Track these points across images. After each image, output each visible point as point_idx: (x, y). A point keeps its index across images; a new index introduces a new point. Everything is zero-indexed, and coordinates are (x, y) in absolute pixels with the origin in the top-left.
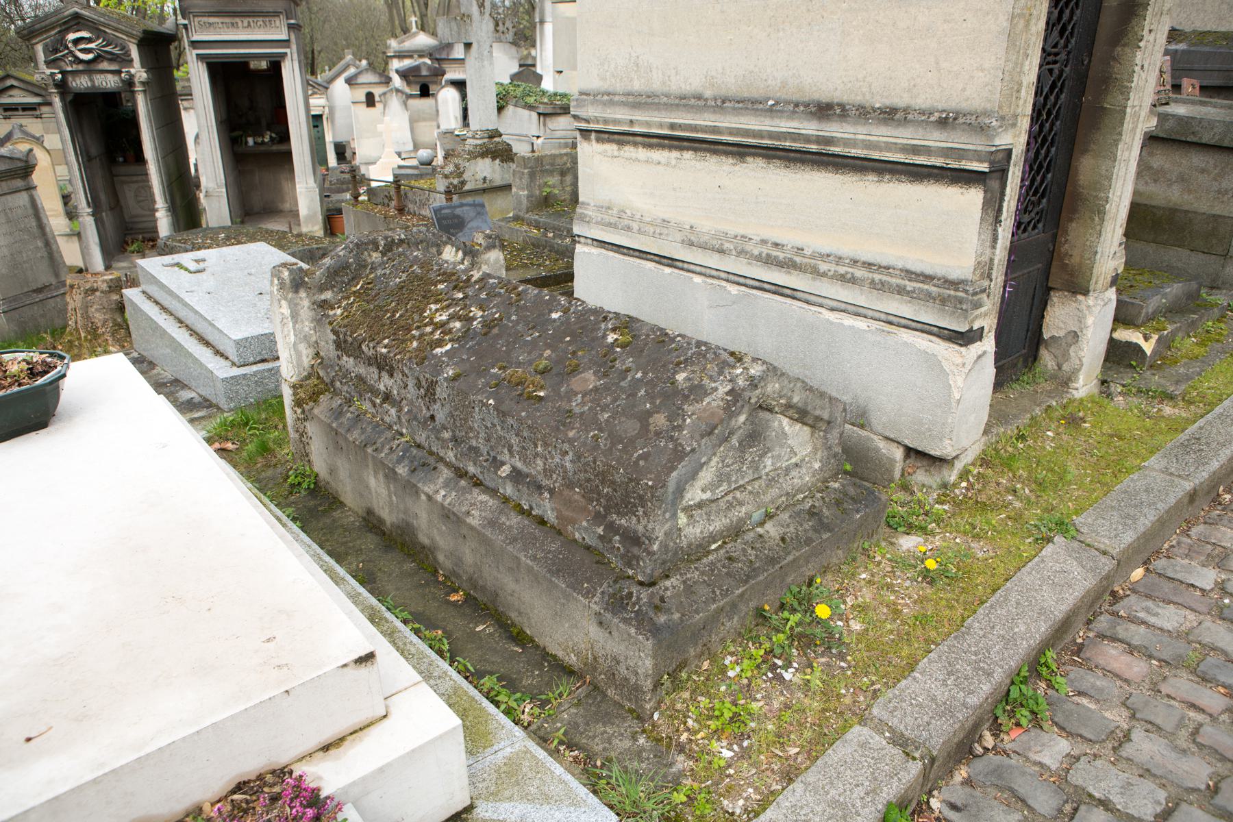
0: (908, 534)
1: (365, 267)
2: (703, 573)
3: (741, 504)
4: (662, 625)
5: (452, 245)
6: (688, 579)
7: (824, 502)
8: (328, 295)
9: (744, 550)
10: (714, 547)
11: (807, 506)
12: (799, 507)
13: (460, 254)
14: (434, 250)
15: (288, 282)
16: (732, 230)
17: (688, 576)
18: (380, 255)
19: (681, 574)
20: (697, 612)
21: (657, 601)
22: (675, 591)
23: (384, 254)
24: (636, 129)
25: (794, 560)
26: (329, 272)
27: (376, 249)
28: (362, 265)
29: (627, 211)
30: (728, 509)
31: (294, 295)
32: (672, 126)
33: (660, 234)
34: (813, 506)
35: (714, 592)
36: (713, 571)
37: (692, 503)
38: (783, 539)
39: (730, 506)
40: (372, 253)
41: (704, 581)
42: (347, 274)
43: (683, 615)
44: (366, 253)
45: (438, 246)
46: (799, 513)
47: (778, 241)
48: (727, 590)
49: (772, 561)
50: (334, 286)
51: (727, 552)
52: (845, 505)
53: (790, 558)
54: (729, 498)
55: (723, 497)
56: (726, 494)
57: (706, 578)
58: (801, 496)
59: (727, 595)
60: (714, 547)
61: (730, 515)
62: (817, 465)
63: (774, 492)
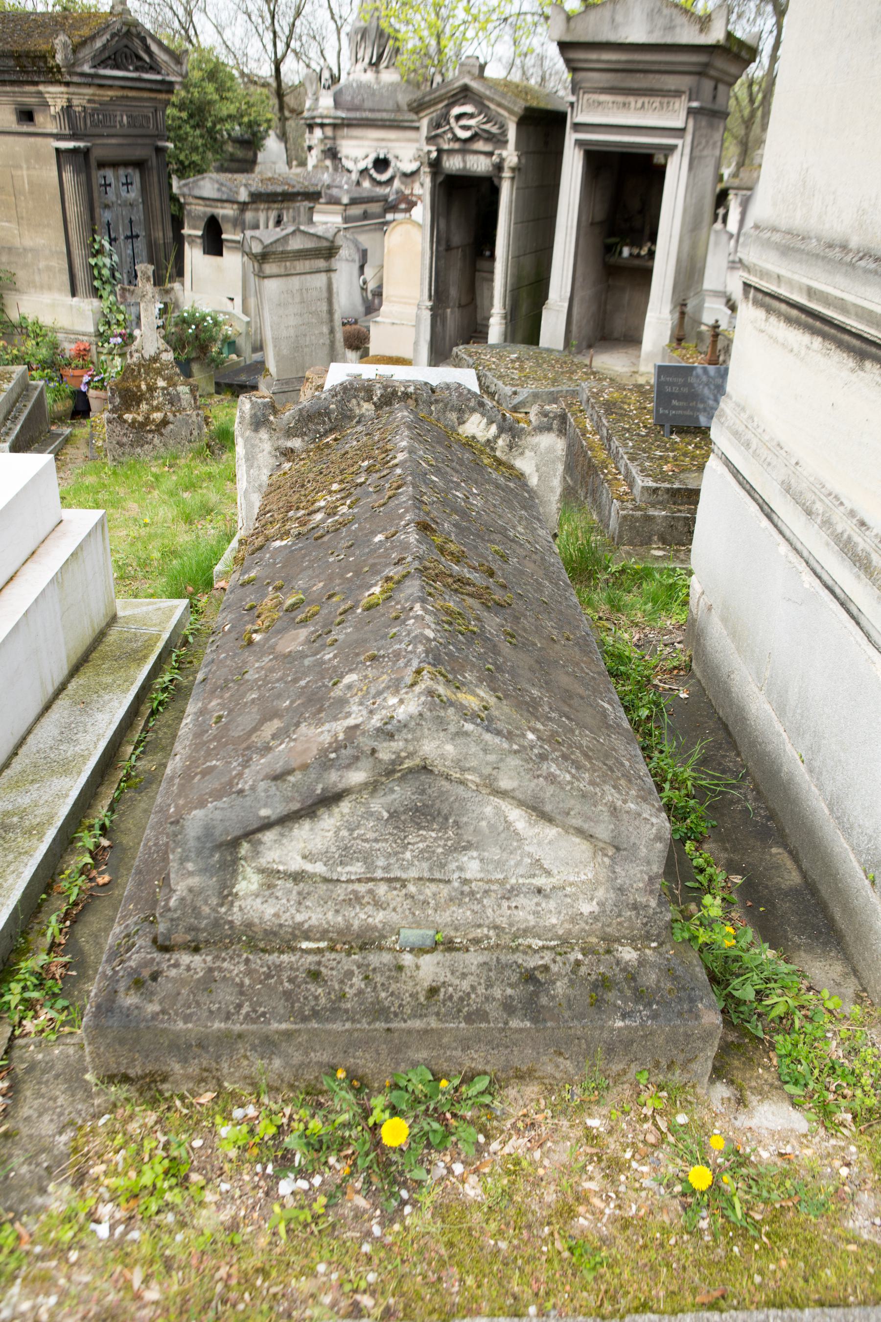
0: (794, 1105)
1: (351, 418)
2: (249, 972)
3: (378, 905)
4: (120, 1007)
5: (483, 415)
6: (220, 969)
7: (573, 972)
8: (296, 443)
9: (350, 974)
10: (305, 945)
11: (533, 962)
12: (519, 958)
13: (494, 429)
14: (453, 416)
15: (247, 416)
16: (835, 485)
17: (225, 965)
18: (373, 407)
19: (217, 957)
20: (187, 1019)
21: (146, 973)
22: (185, 974)
23: (378, 407)
24: (783, 292)
25: (426, 1032)
26: (301, 415)
27: (369, 399)
28: (346, 416)
29: (756, 419)
30: (349, 902)
31: (253, 434)
32: (811, 292)
33: (769, 464)
34: (546, 968)
35: (239, 1006)
36: (268, 976)
37: (281, 868)
38: (433, 991)
39: (356, 899)
40: (362, 402)
41: (242, 984)
42: (324, 423)
43: (163, 1012)
44: (354, 401)
45: (460, 411)
46: (502, 967)
47: (867, 520)
48: (263, 1014)
49: (379, 1012)
50: (305, 434)
51: (319, 963)
52: (610, 996)
53: (417, 1024)
54: (362, 888)
55: (349, 881)
56: (359, 880)
57: (247, 981)
58: (537, 943)
59: (254, 1021)
60: (305, 945)
61: (350, 913)
62: (587, 908)
63: (462, 914)
